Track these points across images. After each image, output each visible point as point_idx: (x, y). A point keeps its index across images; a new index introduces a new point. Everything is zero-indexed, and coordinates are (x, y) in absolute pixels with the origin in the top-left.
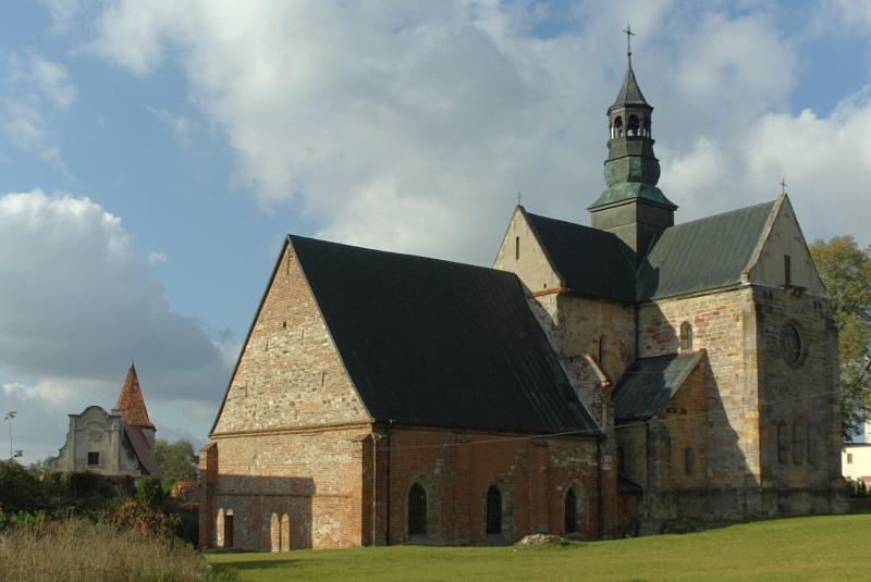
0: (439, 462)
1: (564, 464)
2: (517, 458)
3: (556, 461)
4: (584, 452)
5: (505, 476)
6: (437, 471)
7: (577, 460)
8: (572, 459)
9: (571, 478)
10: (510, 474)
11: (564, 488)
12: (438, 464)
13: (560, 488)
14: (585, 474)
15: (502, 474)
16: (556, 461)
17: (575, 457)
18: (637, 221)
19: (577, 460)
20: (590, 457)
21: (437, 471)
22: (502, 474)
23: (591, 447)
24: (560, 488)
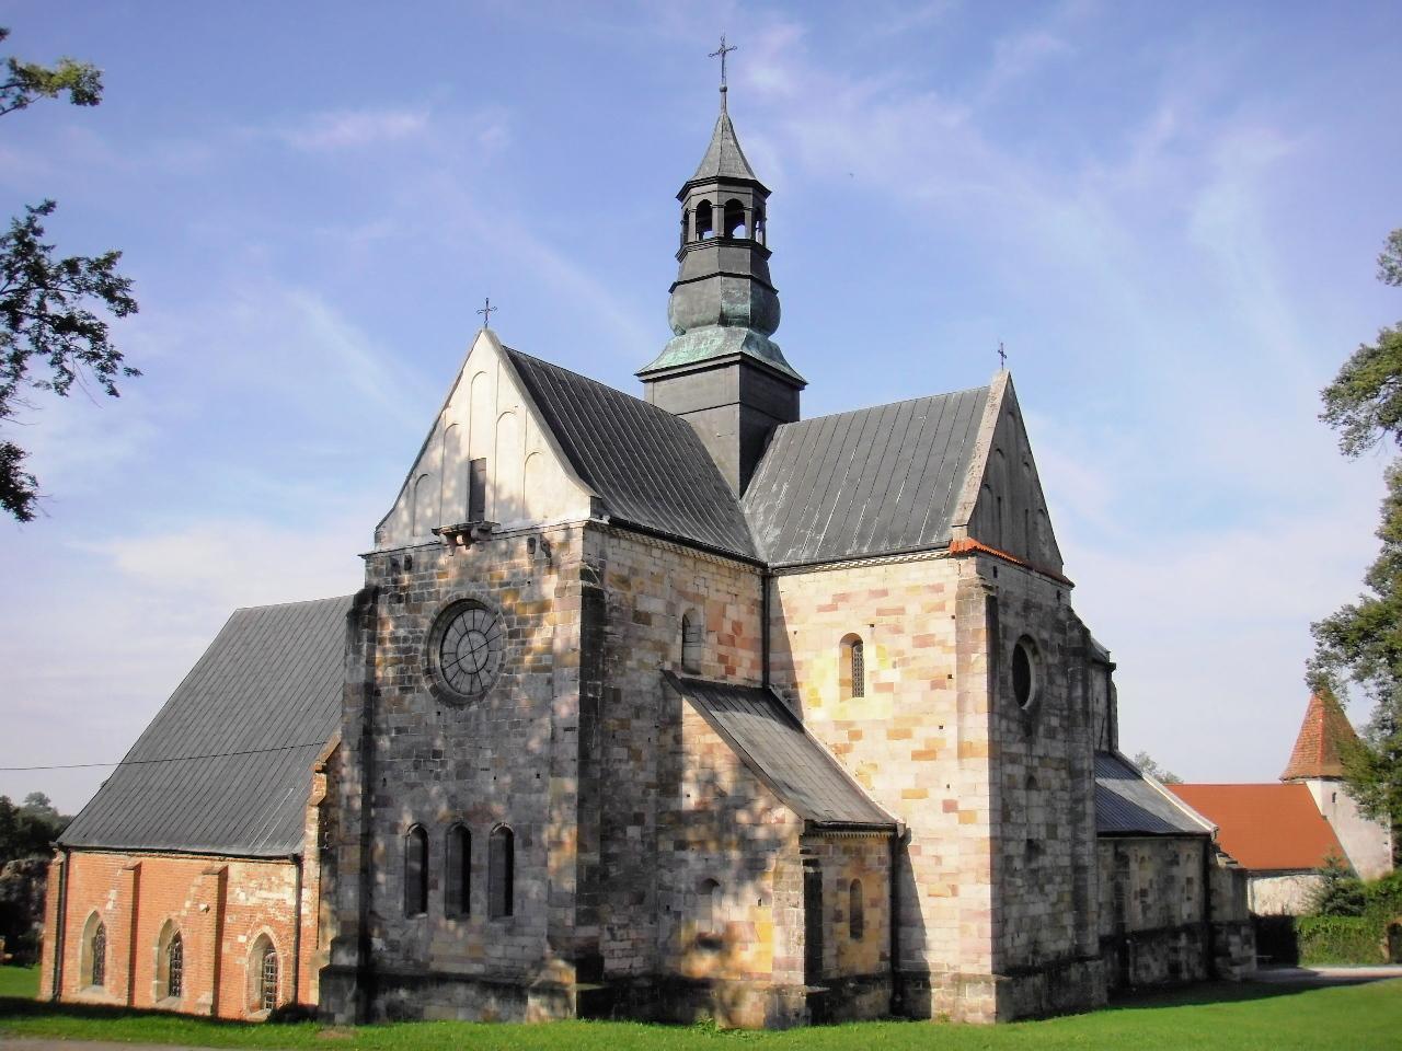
0: (113, 894)
1: (253, 901)
2: (193, 890)
3: (242, 896)
4: (282, 883)
5: (178, 916)
6: (110, 906)
7: (270, 895)
8: (264, 894)
9: (259, 925)
10: (184, 913)
11: (249, 938)
12: (110, 897)
13: (242, 939)
14: (282, 919)
15: (175, 914)
16: (242, 896)
17: (270, 889)
18: (744, 403)
19: (270, 895)
20: (291, 890)
21: (110, 906)
22: (175, 914)
23: (289, 872)
24: (242, 939)
